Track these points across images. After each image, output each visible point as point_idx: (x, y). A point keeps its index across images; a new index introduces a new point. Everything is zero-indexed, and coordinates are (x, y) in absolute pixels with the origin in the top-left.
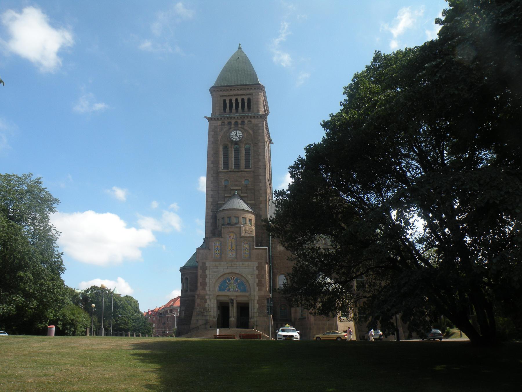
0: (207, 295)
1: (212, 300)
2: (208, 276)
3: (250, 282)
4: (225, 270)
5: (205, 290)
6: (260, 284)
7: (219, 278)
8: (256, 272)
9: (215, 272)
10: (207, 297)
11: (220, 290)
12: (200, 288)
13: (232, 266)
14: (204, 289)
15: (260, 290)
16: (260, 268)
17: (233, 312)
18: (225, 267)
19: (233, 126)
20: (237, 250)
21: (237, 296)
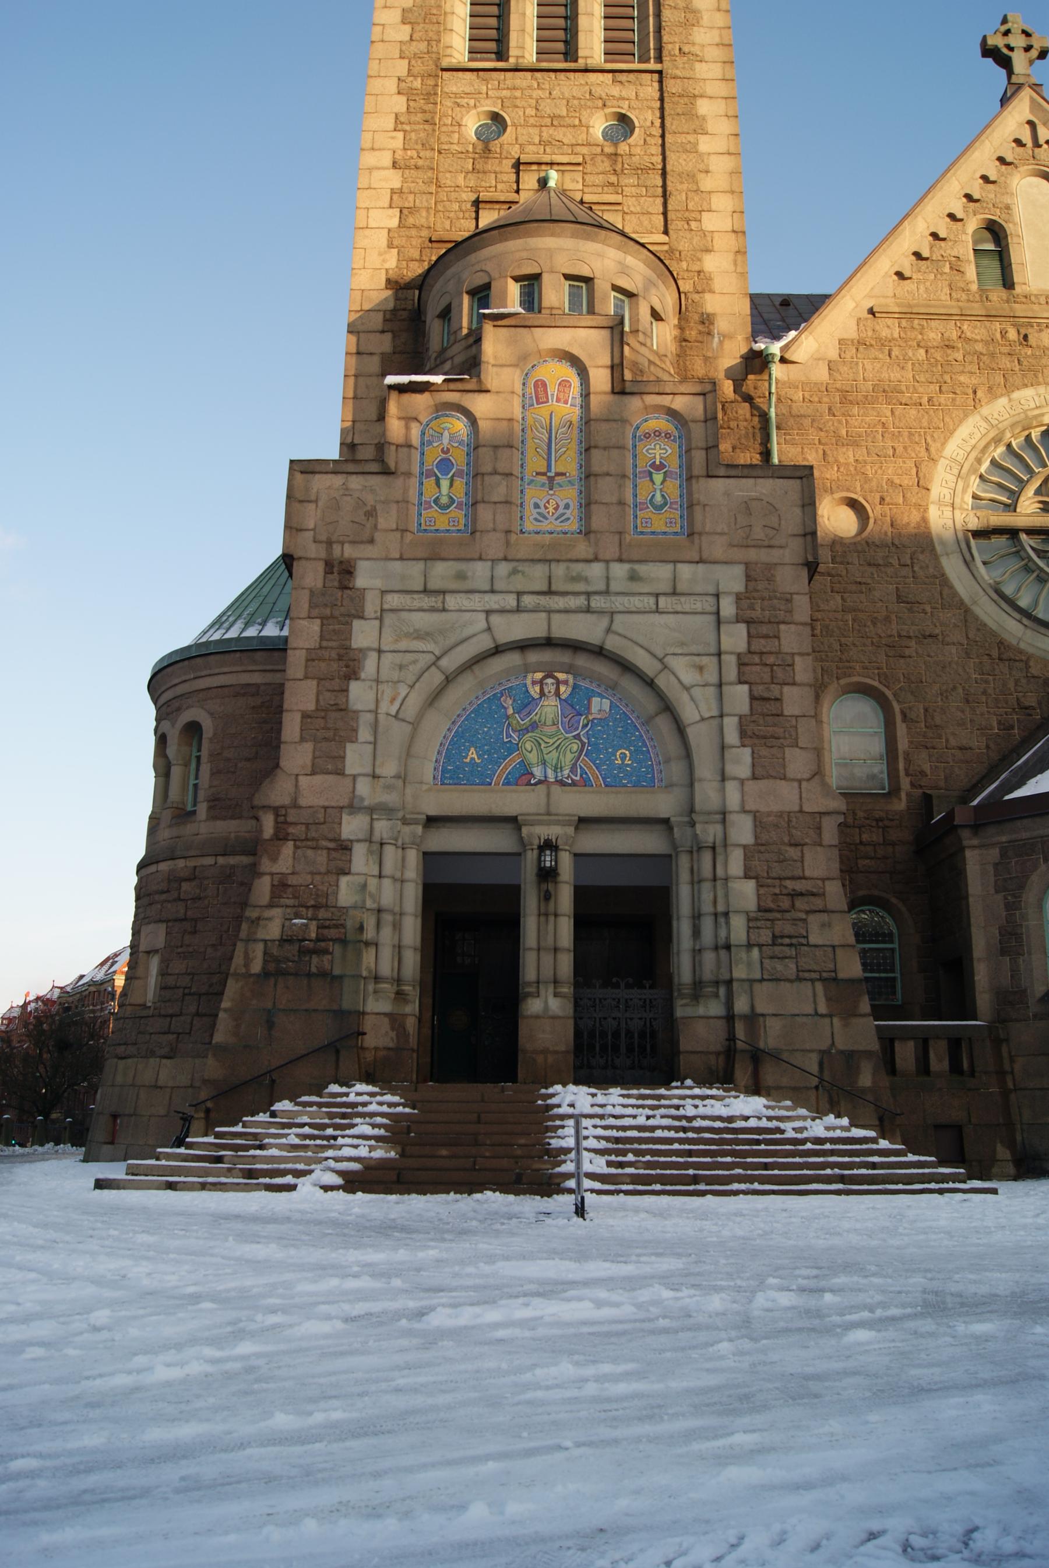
3: (689, 713)
4: (495, 619)
5: (340, 773)
8: (735, 638)
9: (419, 635)
12: (296, 755)
13: (550, 592)
14: (329, 763)
17: (548, 943)
18: (493, 601)
20: (588, 476)
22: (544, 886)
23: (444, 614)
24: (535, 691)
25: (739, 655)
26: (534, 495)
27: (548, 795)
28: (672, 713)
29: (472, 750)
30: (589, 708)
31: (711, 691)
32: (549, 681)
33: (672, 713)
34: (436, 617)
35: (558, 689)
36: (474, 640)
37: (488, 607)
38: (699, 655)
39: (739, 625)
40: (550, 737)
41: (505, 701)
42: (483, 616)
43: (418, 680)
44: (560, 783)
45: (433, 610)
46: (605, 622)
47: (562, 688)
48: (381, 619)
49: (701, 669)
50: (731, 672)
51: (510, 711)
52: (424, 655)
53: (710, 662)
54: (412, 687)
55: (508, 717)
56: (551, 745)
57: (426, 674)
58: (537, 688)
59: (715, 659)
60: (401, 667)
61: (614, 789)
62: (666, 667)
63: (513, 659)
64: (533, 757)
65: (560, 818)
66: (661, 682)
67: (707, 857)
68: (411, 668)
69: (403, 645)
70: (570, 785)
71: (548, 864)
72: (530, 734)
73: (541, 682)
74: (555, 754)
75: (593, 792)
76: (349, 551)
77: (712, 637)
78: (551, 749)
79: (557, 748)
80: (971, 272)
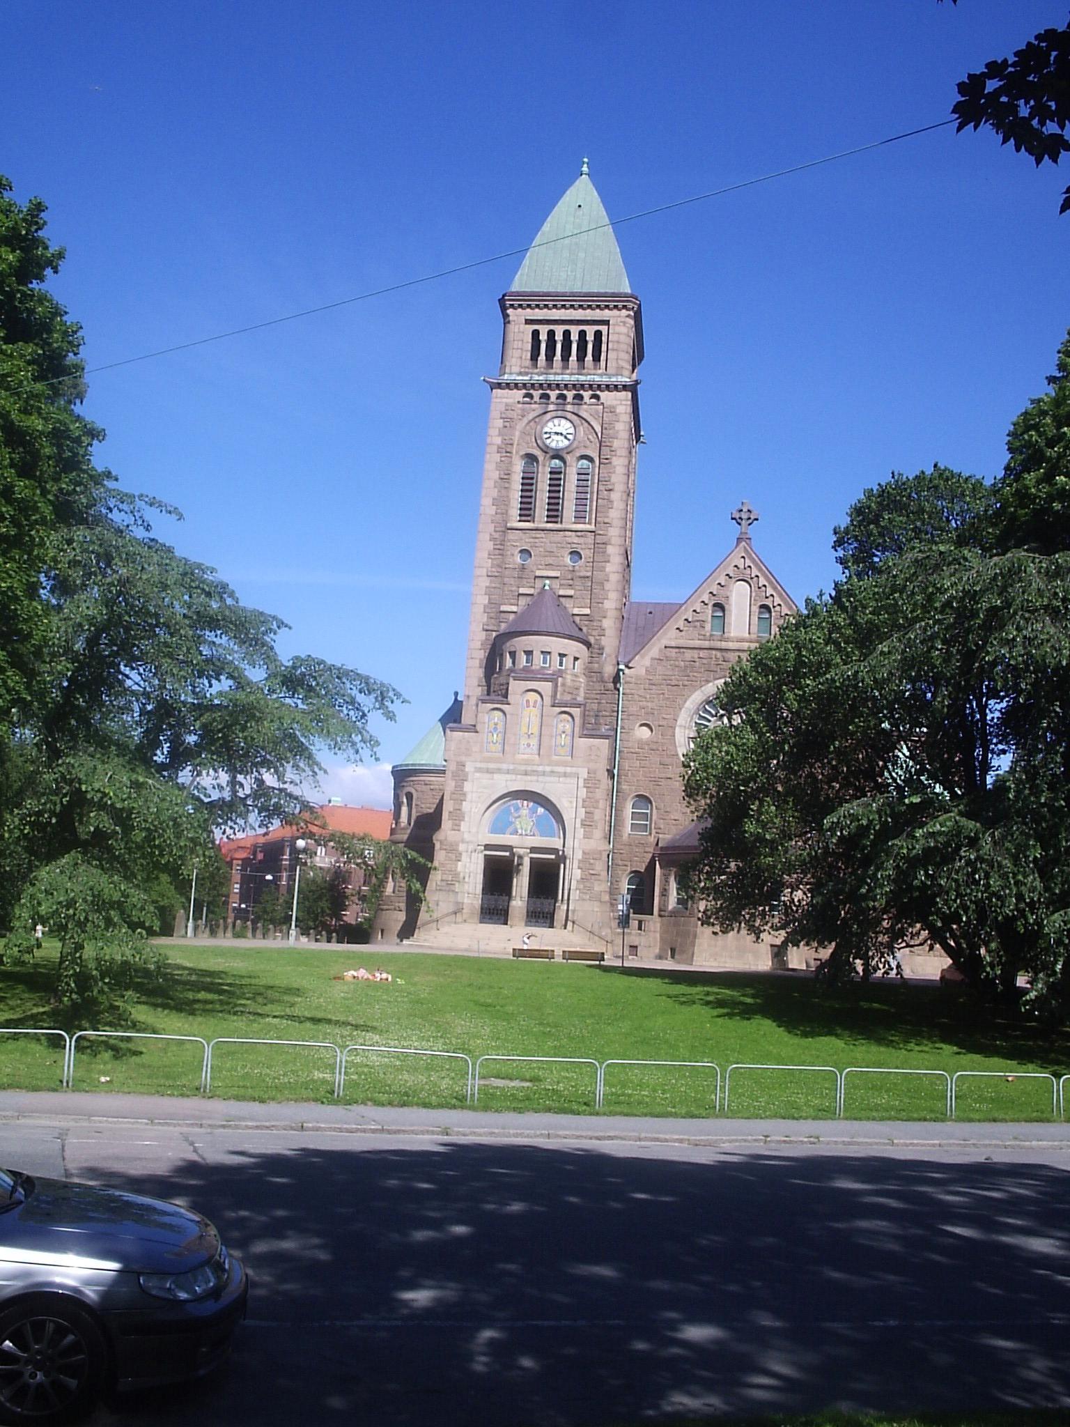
0: (463, 841)
2: (469, 797)
6: (588, 824)
8: (583, 793)
10: (462, 847)
14: (456, 828)
15: (587, 836)
16: (591, 784)
17: (521, 884)
18: (508, 777)
19: (551, 407)
21: (533, 850)
26: (524, 741)
44: (526, 837)
50: (580, 804)
76: (463, 758)
80: (708, 626)
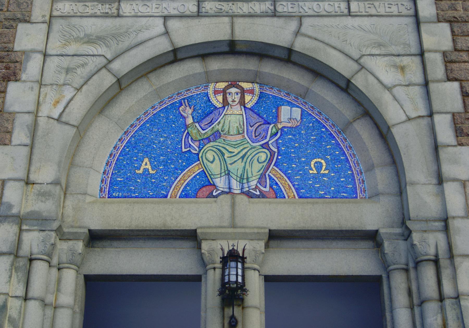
1: (40, 268)
2: (33, 67)
3: (392, 113)
4: (173, 24)
7: (122, 84)
9: (90, 40)
11: (119, 185)
22: (228, 312)
23: (118, 19)
24: (217, 101)
25: (444, 54)
27: (233, 205)
28: (371, 118)
29: (146, 160)
30: (277, 116)
31: (417, 91)
32: (233, 90)
33: (371, 118)
34: (109, 23)
35: (243, 98)
36: (151, 43)
37: (166, 13)
38: (399, 55)
39: (440, 24)
40: (234, 146)
41: (184, 111)
42: (161, 21)
43: (86, 83)
45: (106, 16)
46: (293, 25)
47: (248, 97)
48: (50, 25)
49: (402, 69)
50: (437, 69)
51: (190, 121)
52: (94, 59)
53: (413, 63)
54: (78, 90)
55: (186, 127)
56: (234, 150)
57: (95, 77)
58: (220, 98)
59: (417, 60)
60: (68, 70)
61: (309, 200)
62: (363, 67)
63: (194, 67)
64: (215, 168)
65: (247, 231)
66: (359, 82)
67: (429, 273)
68: (79, 71)
69: (73, 48)
70: (258, 197)
71: (233, 278)
72: (212, 144)
73: (224, 92)
74: (240, 165)
75: (285, 203)
77: (412, 38)
78: (235, 159)
79: (243, 158)
